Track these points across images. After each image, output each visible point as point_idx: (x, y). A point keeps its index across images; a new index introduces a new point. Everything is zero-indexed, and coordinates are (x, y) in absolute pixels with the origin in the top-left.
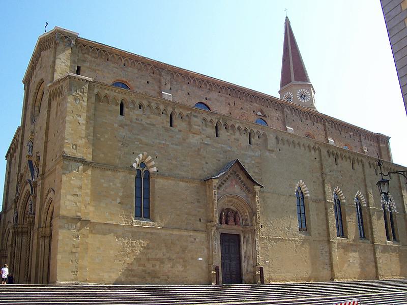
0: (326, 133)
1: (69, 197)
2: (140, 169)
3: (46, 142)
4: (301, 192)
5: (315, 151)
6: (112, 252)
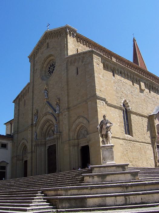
3: (67, 90)
6: (119, 154)
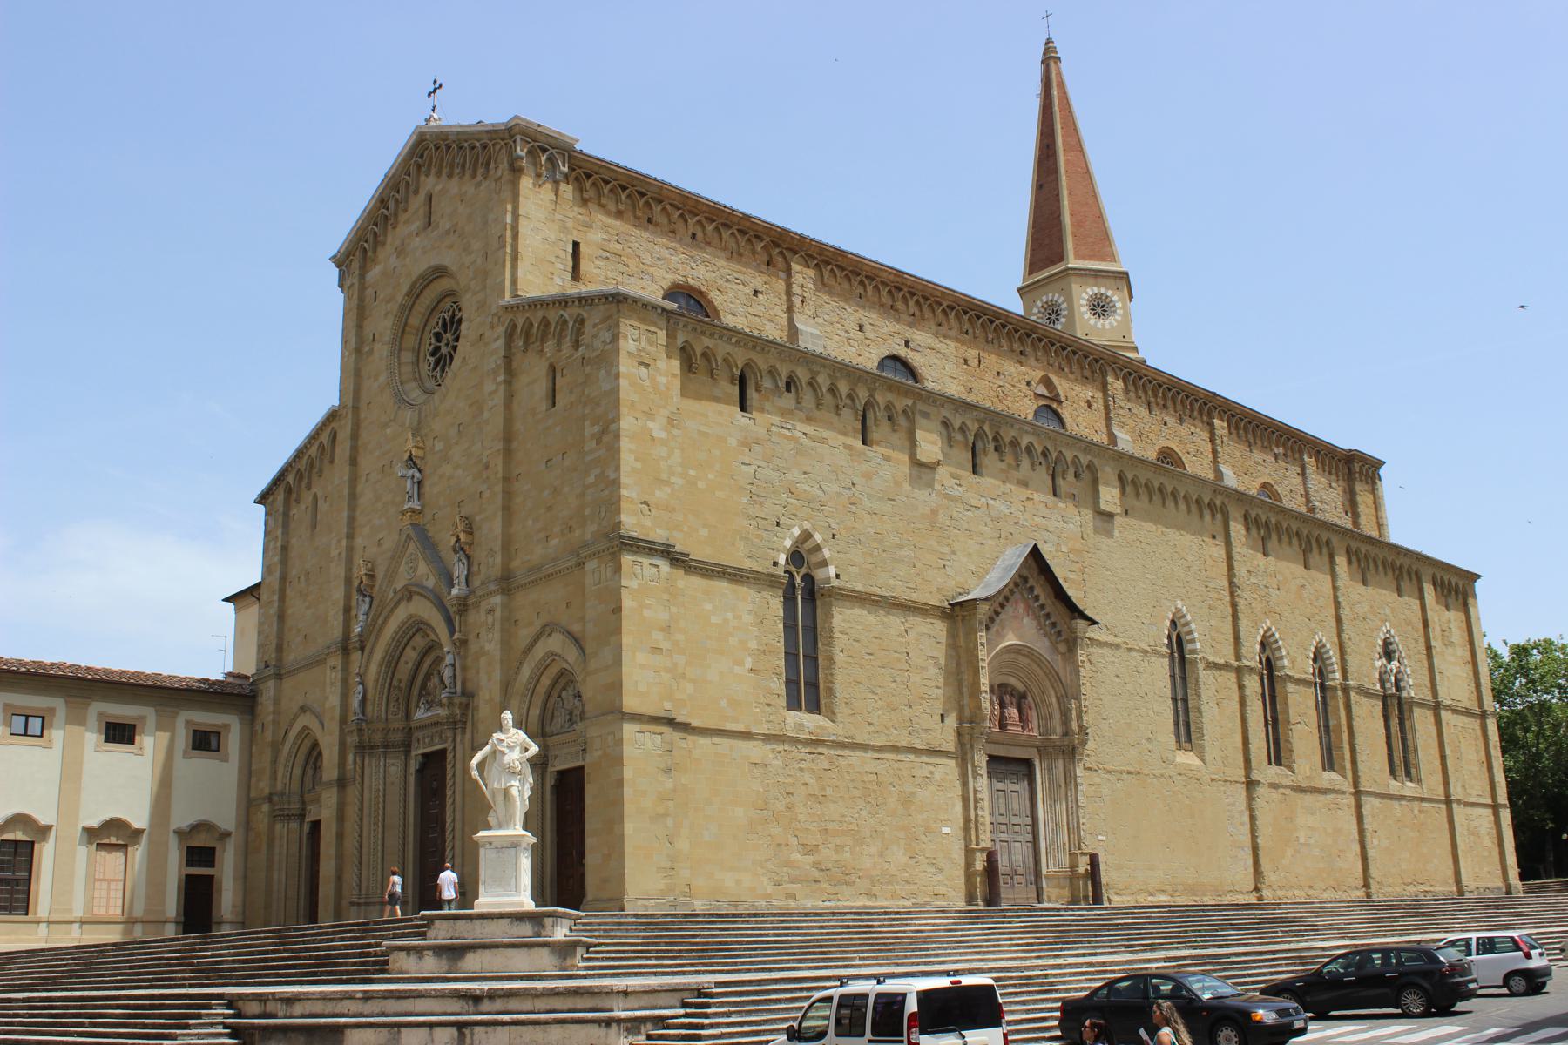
0: (1215, 452)
1: (642, 657)
2: (792, 569)
4: (1179, 636)
5: (1213, 516)
